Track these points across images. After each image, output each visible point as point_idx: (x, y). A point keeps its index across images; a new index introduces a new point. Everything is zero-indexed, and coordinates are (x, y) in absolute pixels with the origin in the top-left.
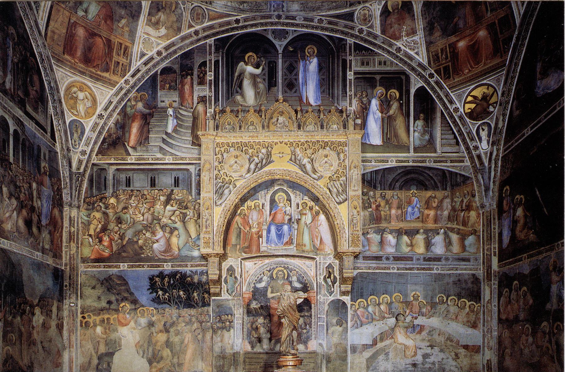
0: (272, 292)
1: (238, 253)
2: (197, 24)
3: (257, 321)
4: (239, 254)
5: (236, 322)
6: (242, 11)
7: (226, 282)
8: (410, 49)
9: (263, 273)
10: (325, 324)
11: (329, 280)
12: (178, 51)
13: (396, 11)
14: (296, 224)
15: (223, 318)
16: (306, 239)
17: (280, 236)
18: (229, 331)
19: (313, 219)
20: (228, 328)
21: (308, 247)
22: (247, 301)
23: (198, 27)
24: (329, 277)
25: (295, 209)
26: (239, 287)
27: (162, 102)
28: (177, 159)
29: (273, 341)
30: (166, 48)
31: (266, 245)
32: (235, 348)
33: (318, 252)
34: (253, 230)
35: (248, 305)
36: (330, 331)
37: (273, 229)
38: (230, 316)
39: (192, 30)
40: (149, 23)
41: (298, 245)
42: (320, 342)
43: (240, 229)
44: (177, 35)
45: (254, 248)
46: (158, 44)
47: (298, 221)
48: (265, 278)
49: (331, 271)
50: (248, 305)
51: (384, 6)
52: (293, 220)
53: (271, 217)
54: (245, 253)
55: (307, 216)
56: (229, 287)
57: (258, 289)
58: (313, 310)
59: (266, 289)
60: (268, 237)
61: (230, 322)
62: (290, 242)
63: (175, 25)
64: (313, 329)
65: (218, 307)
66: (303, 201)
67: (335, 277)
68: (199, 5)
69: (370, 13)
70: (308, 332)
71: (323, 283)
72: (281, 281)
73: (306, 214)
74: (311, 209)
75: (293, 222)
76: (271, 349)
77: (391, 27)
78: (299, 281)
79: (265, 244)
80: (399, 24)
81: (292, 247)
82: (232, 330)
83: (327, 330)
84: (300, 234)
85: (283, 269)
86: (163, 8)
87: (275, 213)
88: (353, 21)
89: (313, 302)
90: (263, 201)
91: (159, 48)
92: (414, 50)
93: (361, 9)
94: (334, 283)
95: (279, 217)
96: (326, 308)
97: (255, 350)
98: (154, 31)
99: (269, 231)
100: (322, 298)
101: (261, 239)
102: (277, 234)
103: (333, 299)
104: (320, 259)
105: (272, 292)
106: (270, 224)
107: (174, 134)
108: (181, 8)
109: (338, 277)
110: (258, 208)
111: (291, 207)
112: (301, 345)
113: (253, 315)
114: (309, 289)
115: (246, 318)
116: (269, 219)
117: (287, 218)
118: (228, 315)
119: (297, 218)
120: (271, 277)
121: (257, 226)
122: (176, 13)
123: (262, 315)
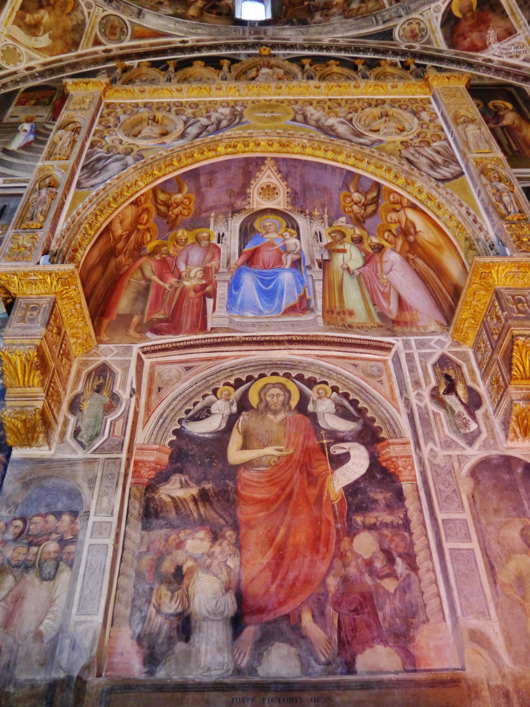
0: (244, 447)
1: (132, 332)
2: (110, 40)
3: (180, 545)
4: (137, 335)
5: (88, 541)
6: (195, 34)
7: (75, 406)
8: (511, 57)
9: (215, 392)
10: (475, 545)
11: (451, 399)
12: (68, 69)
13: (469, 15)
14: (317, 267)
15: (37, 525)
16: (353, 297)
17: (269, 294)
18: (52, 578)
19: (367, 260)
20: (48, 568)
21: (361, 316)
22: (147, 474)
23: (110, 46)
24: (451, 389)
25: (312, 241)
26: (119, 425)
27: (12, 117)
28: (13, 181)
29: (250, 632)
30: (44, 65)
31: (227, 314)
32: (64, 657)
33: (398, 329)
34: (187, 284)
35: (151, 487)
36: (506, 576)
37: (248, 281)
38: (66, 518)
39: (100, 48)
40: (20, 21)
41: (328, 312)
42: (473, 622)
43: (149, 280)
44: (70, 51)
45: (187, 320)
46: (31, 59)
47: (324, 265)
48: (222, 409)
49: (451, 373)
50: (151, 487)
51: (445, 11)
52: (308, 262)
53: (244, 258)
54: (157, 331)
55: (347, 256)
56: (86, 421)
57: (192, 439)
58: (410, 504)
59: (222, 437)
60: (232, 298)
61: (63, 542)
62: (302, 306)
63: (69, 38)
64: (426, 577)
65: (26, 485)
66: (332, 229)
67: (470, 391)
68: (117, 14)
69: (422, 25)
70: (405, 589)
71: (432, 407)
72: (275, 413)
73: (344, 251)
74: (358, 241)
75: (309, 267)
76: (238, 671)
77: (465, 38)
78: (342, 413)
79: (221, 311)
80: (480, 31)
81: (308, 317)
82: (64, 576)
83: (491, 569)
84: (332, 288)
85: (283, 380)
86: (49, 5)
87: (255, 252)
88: (393, 40)
89: (404, 475)
90: (222, 229)
91: (32, 64)
92: (517, 56)
93: (404, 23)
94: (474, 402)
95: (266, 256)
96: (466, 487)
97: (161, 674)
98: (28, 37)
99: (235, 285)
100: (441, 453)
101: (210, 302)
102: (261, 292)
103: (483, 454)
104: (407, 345)
105: (244, 447)
106: (239, 271)
107: (22, 152)
108: (82, 12)
109: (482, 389)
110: (205, 243)
111: (299, 238)
112: (380, 648)
113: (170, 525)
114: (383, 435)
115: (136, 533)
116: (236, 260)
117: (288, 260)
118: (58, 515)
119: (318, 257)
120: (243, 405)
121: (200, 274)
122: (72, 17)
123: (202, 522)
